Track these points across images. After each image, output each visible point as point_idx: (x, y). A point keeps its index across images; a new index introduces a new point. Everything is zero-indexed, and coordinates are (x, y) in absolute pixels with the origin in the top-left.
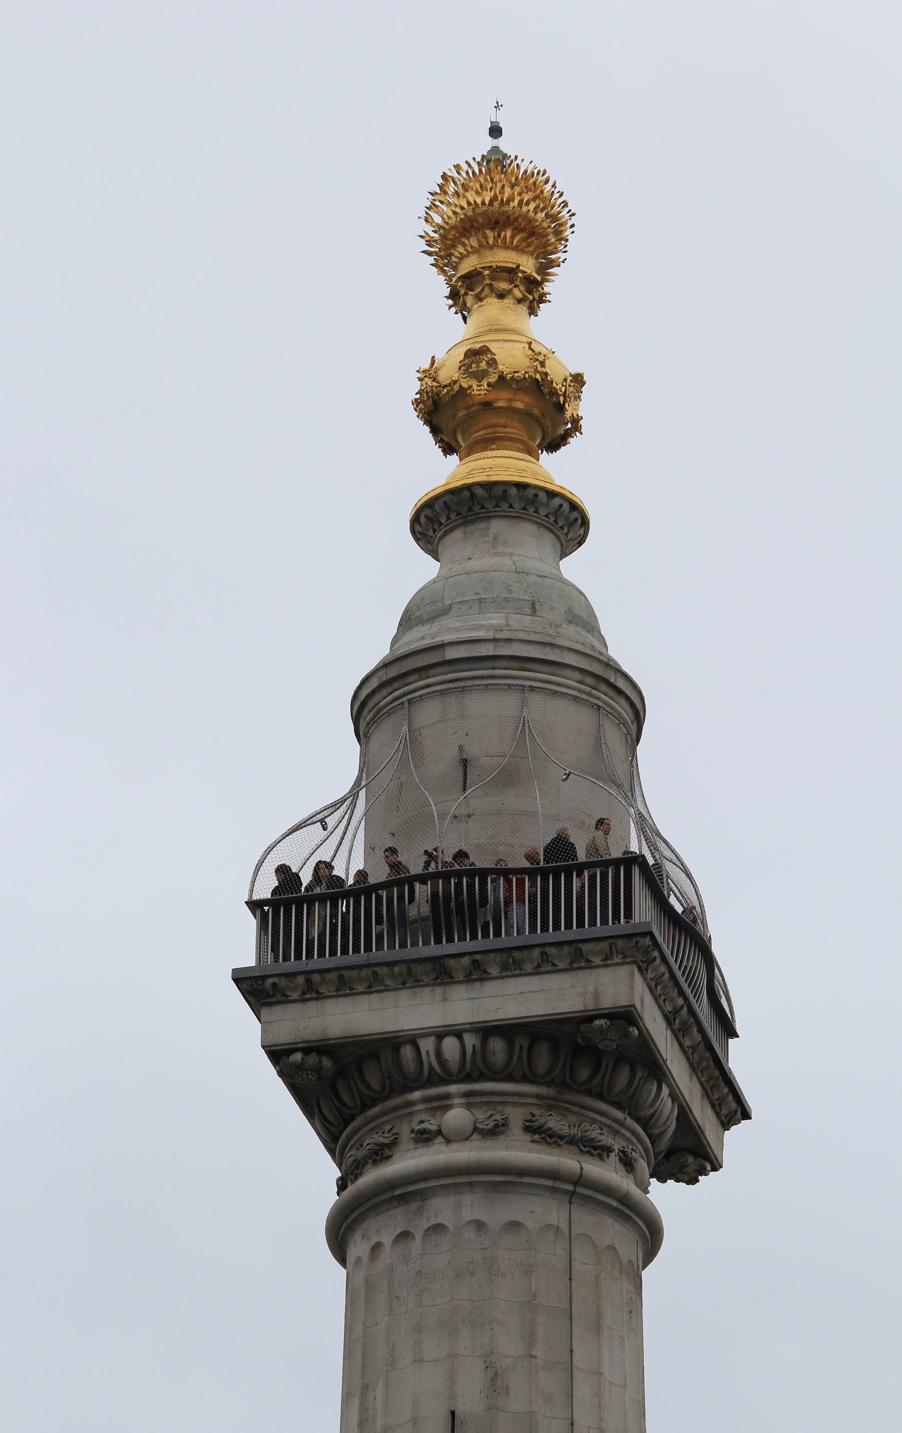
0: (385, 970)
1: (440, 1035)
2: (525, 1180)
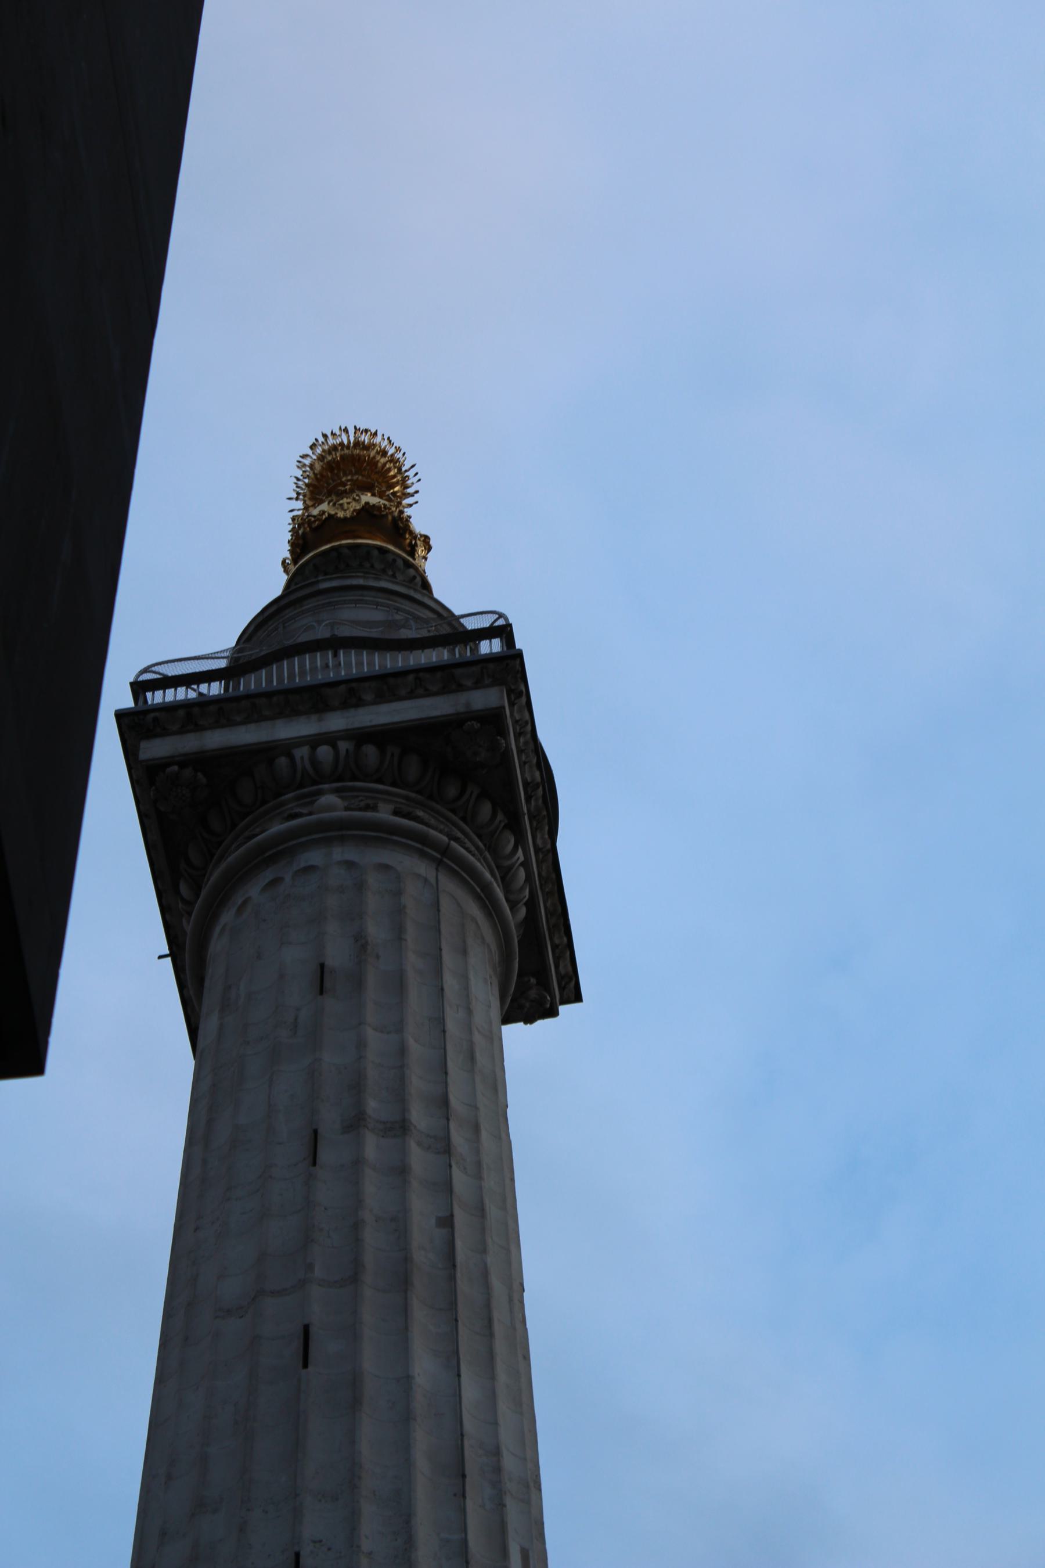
1: (314, 742)
2: (395, 838)
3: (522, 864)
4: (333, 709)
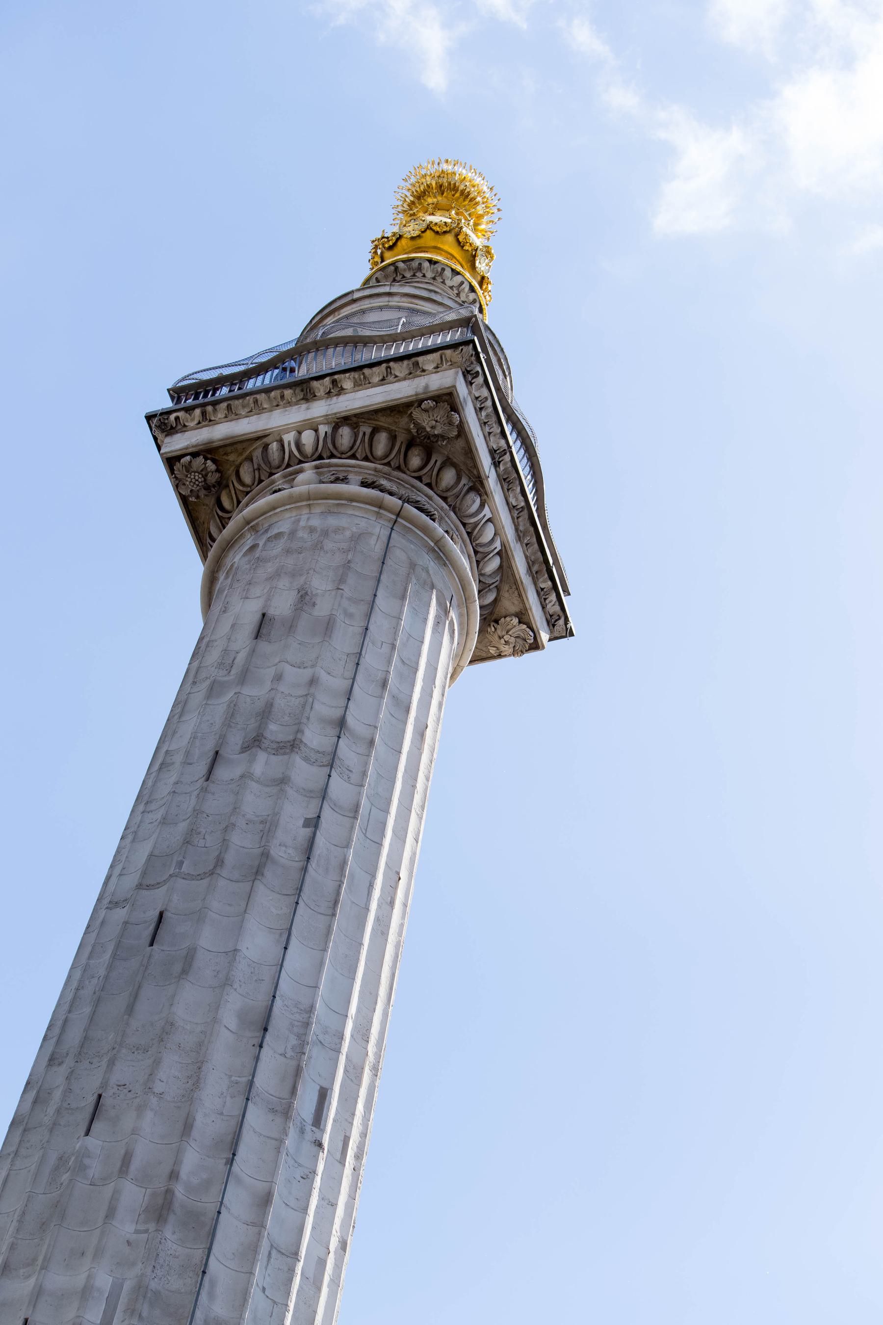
0: (262, 397)
2: (354, 504)
3: (489, 520)
4: (321, 399)
